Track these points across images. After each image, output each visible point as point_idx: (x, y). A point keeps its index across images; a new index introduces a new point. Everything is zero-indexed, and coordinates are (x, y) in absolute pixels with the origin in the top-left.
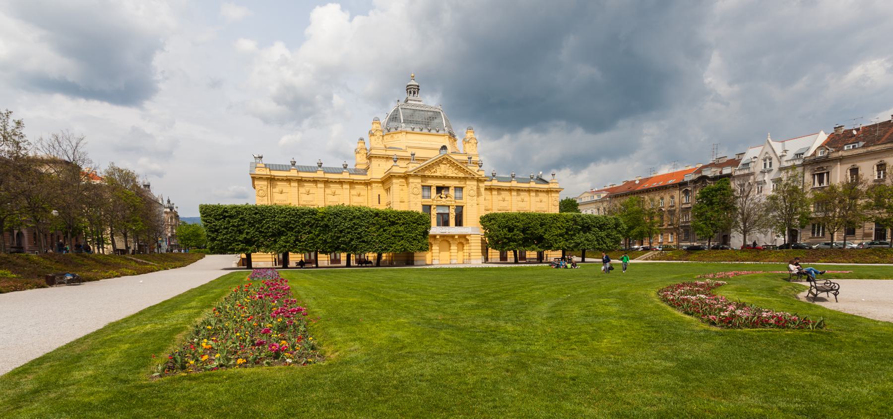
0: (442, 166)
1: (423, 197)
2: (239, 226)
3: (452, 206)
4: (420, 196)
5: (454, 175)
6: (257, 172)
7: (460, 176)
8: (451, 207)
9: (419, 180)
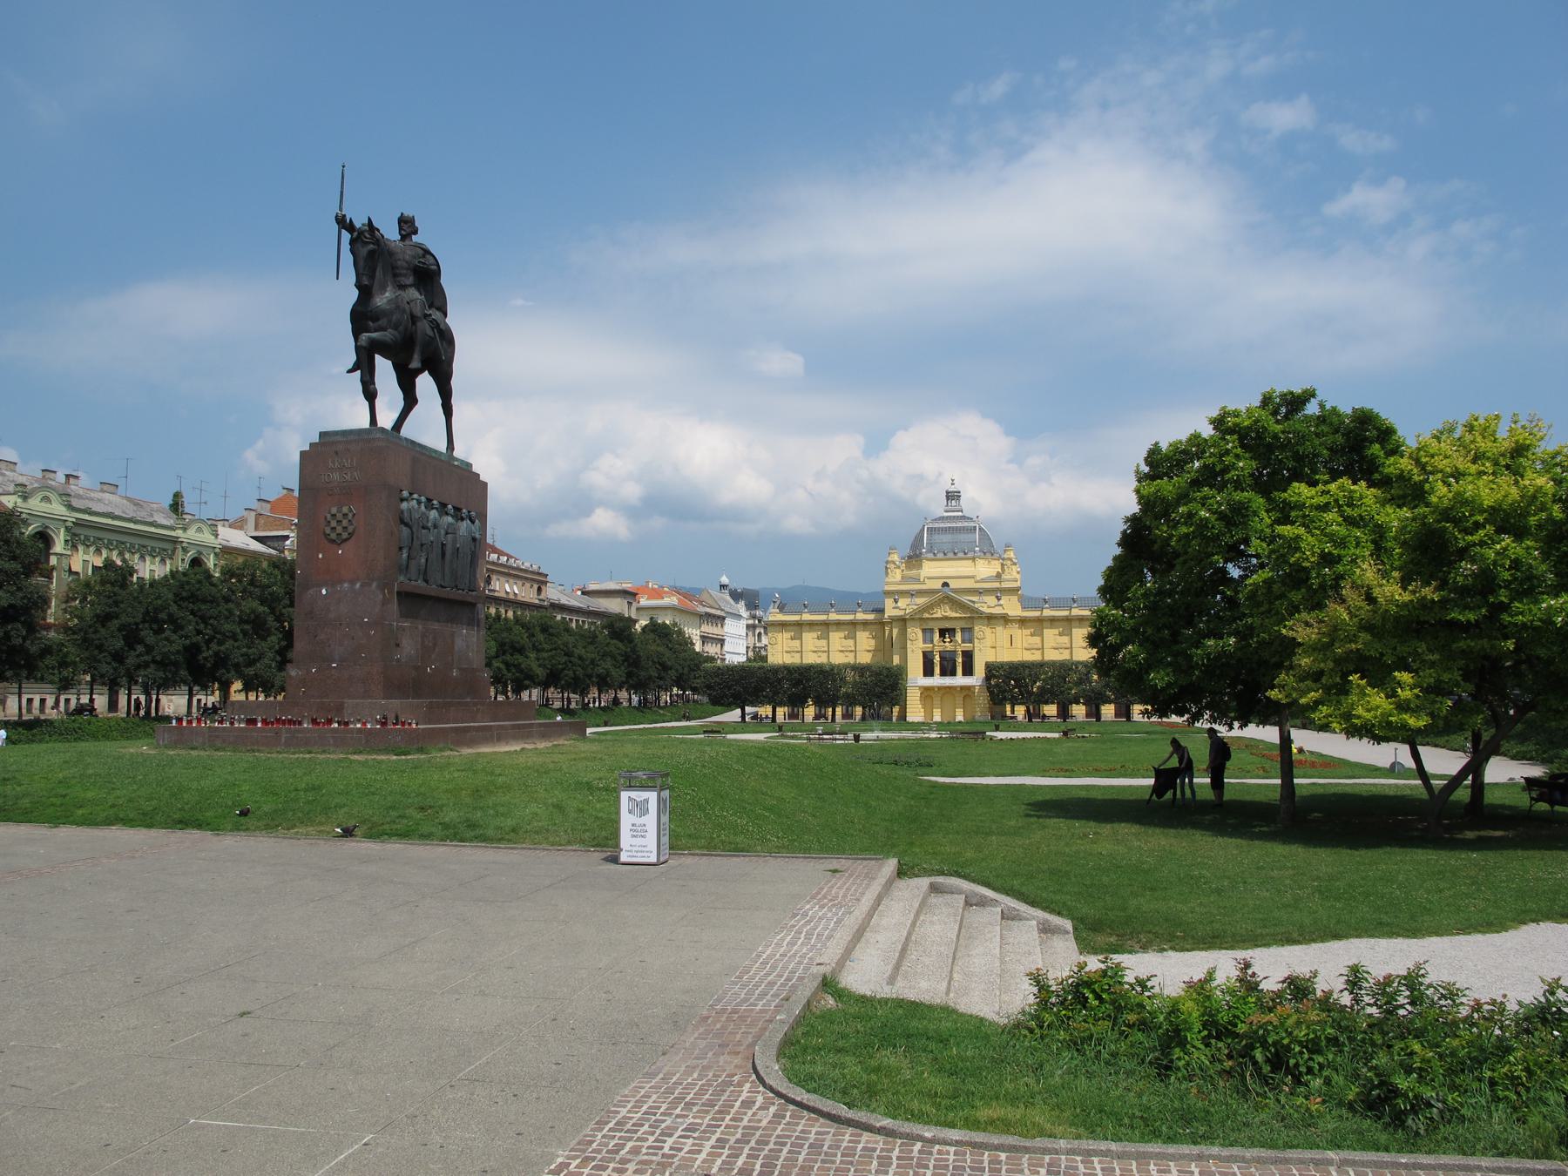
6: (770, 619)
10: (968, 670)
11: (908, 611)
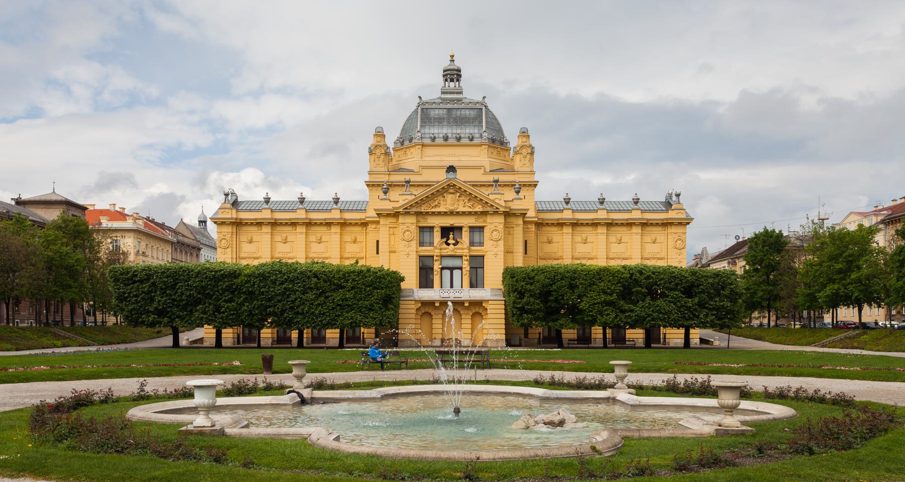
0: (449, 197)
1: (422, 244)
2: (150, 292)
3: (466, 256)
4: (414, 244)
5: (467, 209)
6: (219, 217)
7: (477, 209)
8: (464, 258)
9: (411, 220)
10: (476, 283)
11: (401, 203)
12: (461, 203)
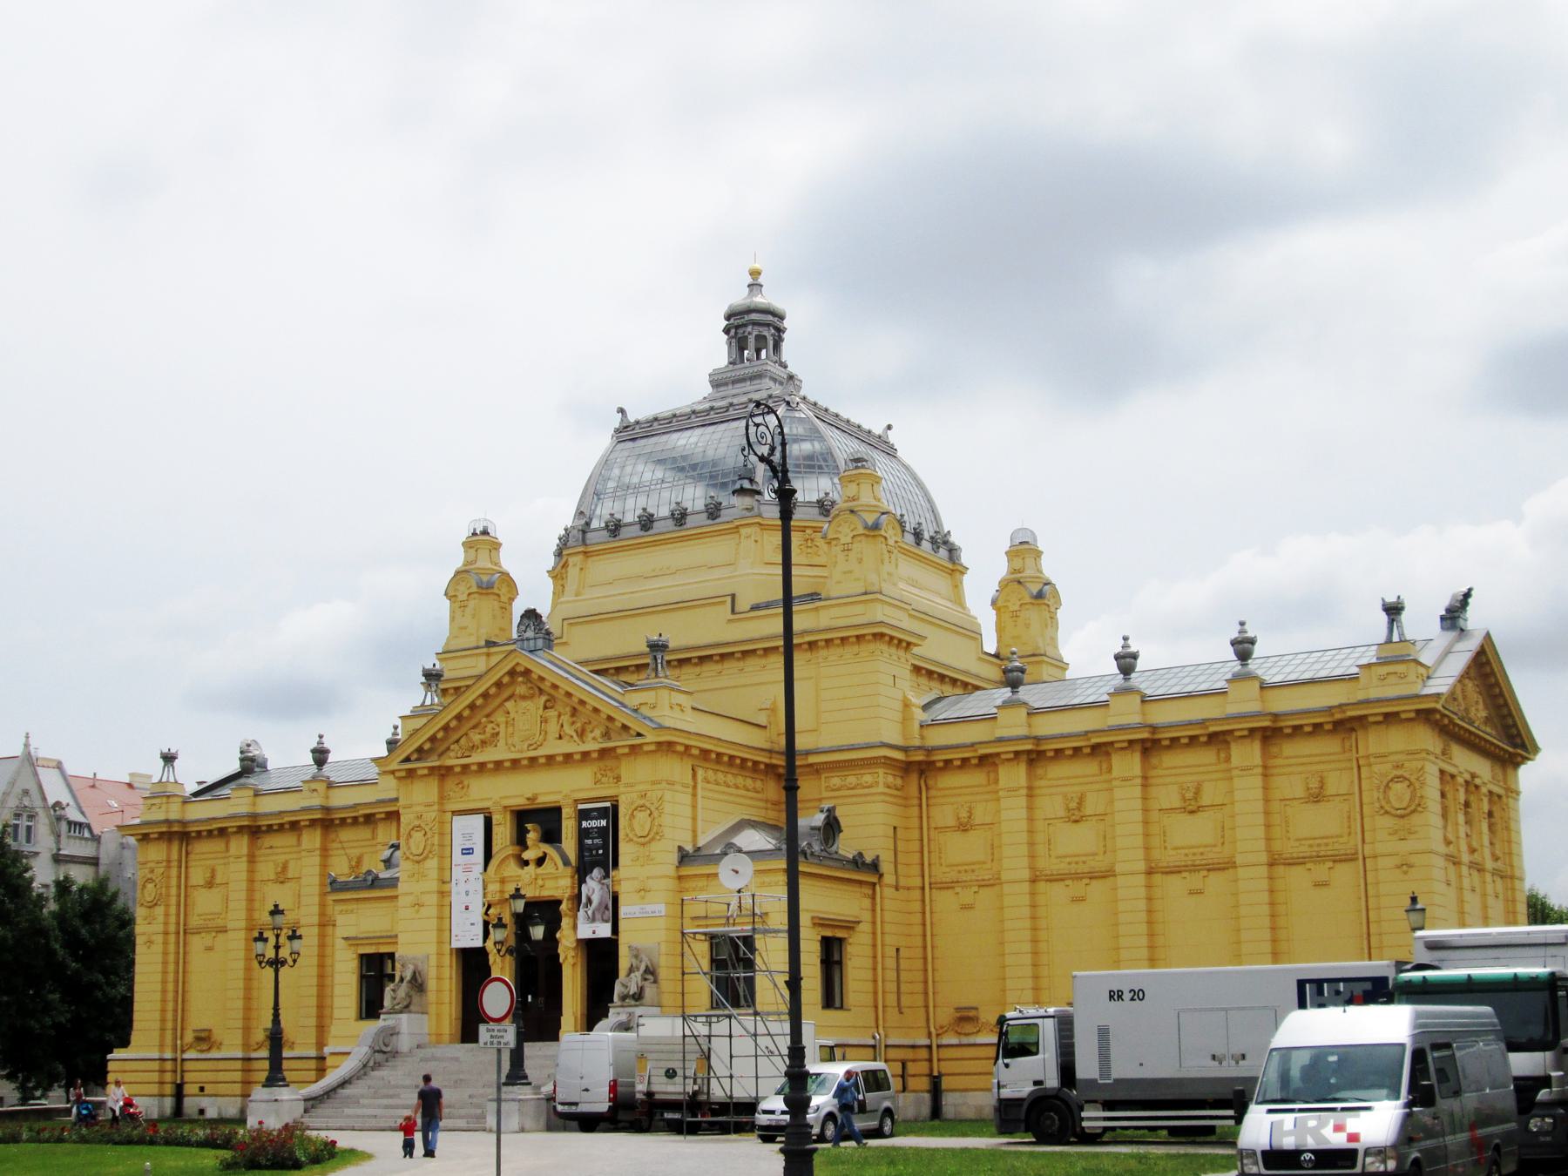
12: (553, 728)
